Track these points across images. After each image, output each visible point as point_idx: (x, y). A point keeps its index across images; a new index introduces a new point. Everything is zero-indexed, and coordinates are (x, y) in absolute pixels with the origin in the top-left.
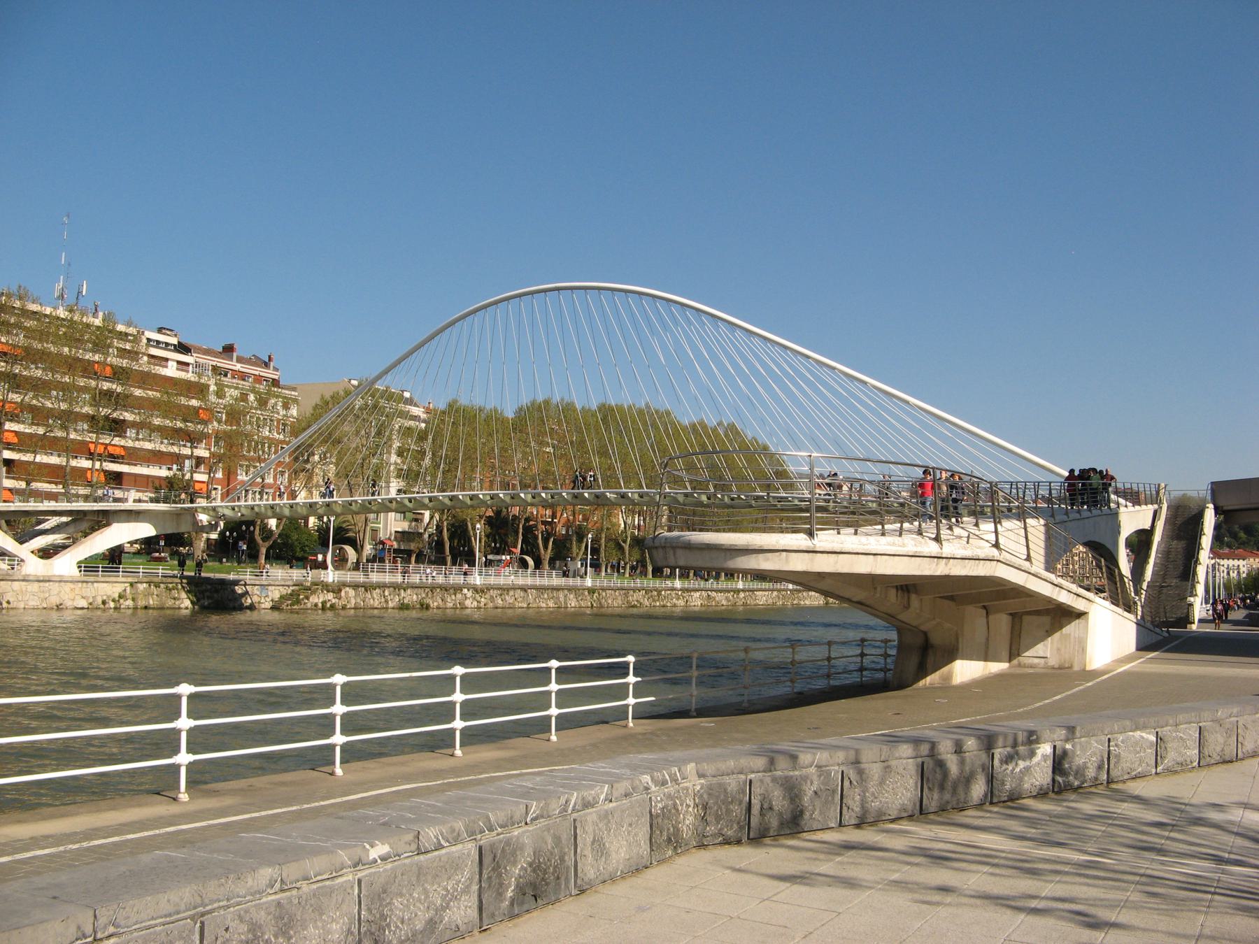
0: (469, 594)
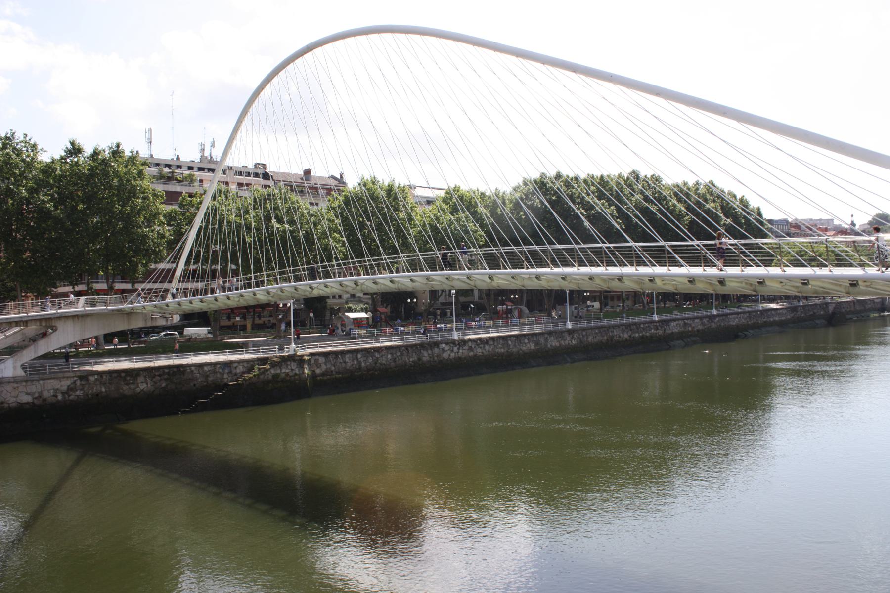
0: (447, 348)
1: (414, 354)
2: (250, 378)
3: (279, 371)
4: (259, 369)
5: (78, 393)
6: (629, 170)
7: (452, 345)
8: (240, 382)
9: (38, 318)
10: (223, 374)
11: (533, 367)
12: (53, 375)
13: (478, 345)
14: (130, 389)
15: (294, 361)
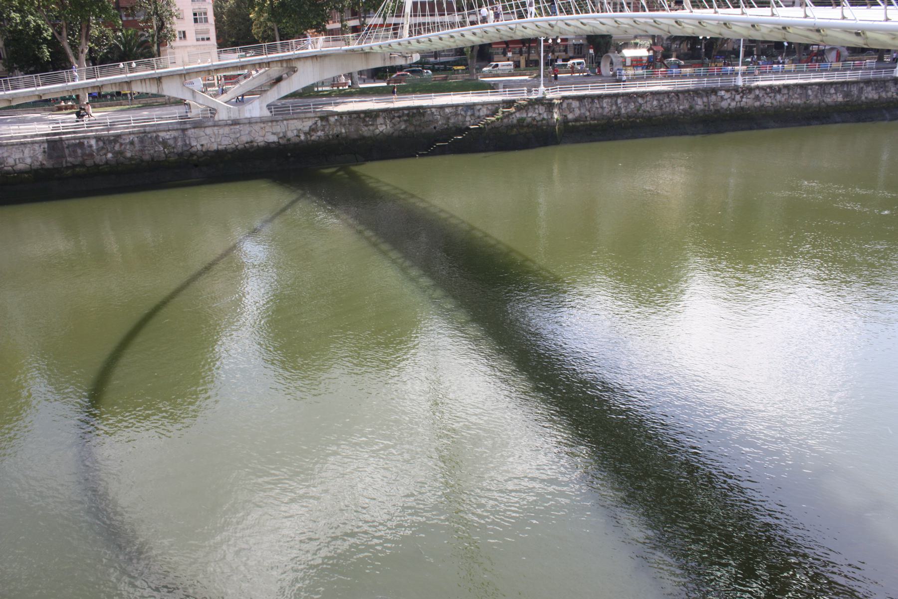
0: (727, 95)
1: (685, 101)
2: (493, 122)
3: (524, 115)
4: (503, 112)
5: (320, 133)
7: (734, 93)
8: (481, 126)
9: (277, 59)
10: (465, 117)
11: (836, 123)
12: (295, 116)
13: (767, 94)
14: (369, 130)
15: (543, 104)
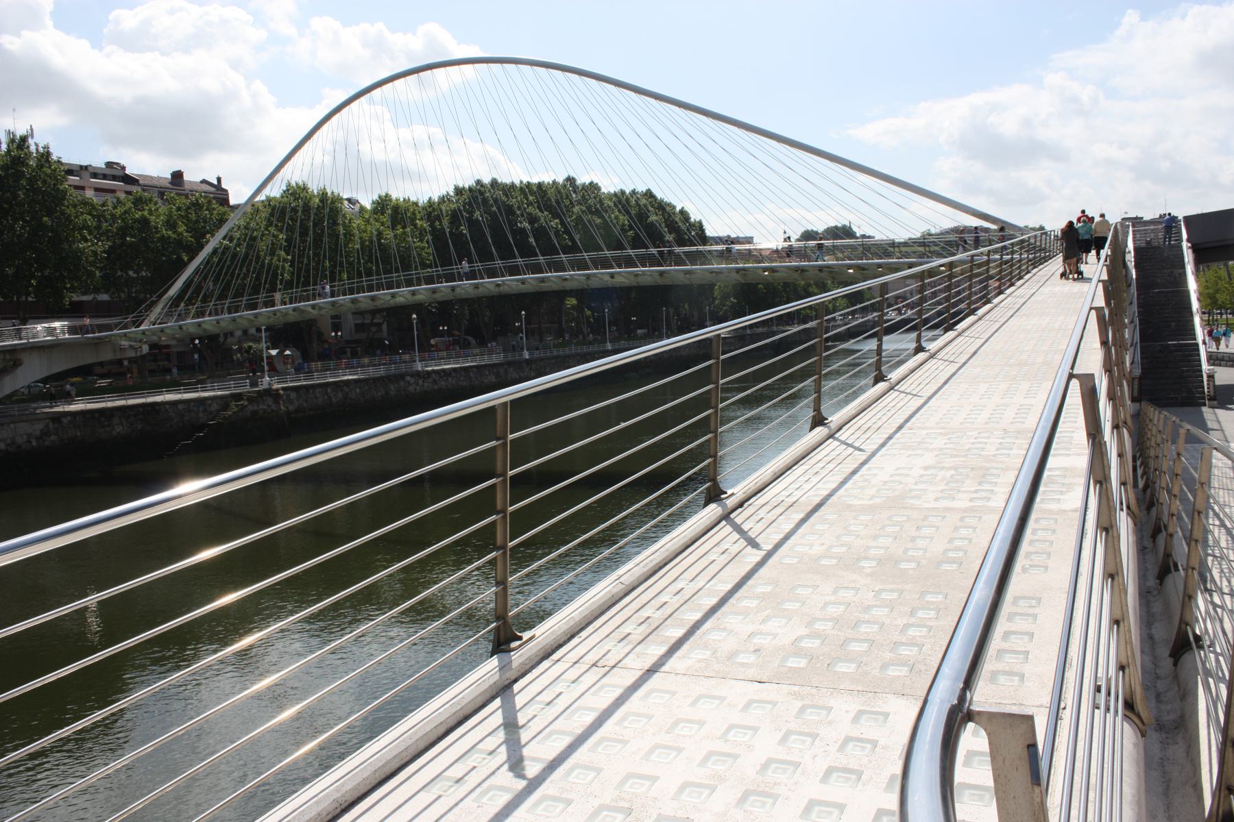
0: (412, 381)
2: (230, 416)
3: (256, 408)
4: (237, 406)
5: (53, 438)
6: (565, 176)
9: (9, 348)
